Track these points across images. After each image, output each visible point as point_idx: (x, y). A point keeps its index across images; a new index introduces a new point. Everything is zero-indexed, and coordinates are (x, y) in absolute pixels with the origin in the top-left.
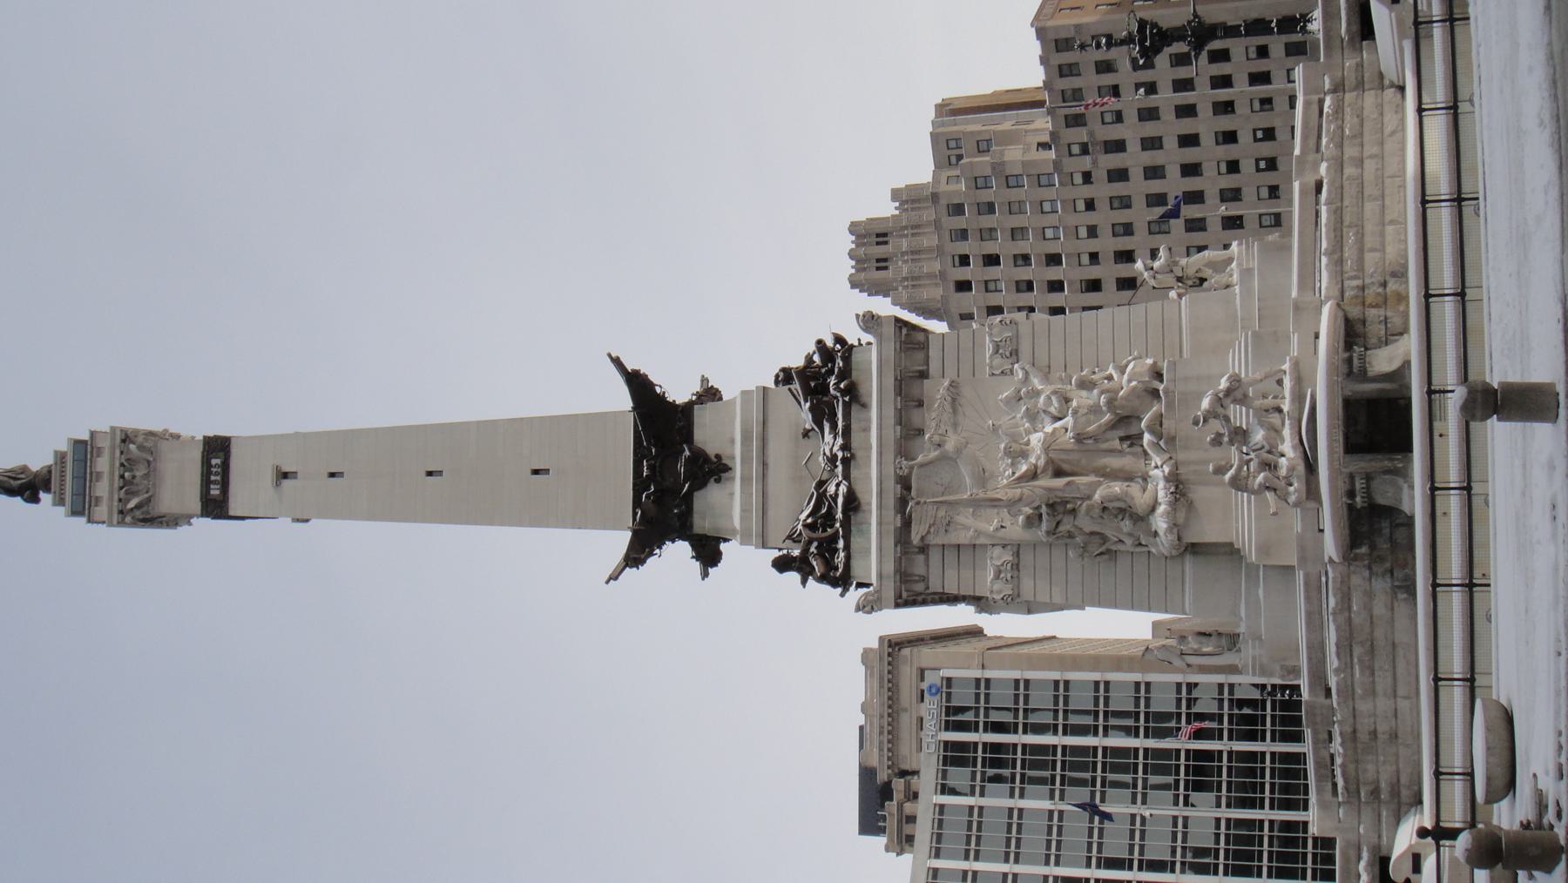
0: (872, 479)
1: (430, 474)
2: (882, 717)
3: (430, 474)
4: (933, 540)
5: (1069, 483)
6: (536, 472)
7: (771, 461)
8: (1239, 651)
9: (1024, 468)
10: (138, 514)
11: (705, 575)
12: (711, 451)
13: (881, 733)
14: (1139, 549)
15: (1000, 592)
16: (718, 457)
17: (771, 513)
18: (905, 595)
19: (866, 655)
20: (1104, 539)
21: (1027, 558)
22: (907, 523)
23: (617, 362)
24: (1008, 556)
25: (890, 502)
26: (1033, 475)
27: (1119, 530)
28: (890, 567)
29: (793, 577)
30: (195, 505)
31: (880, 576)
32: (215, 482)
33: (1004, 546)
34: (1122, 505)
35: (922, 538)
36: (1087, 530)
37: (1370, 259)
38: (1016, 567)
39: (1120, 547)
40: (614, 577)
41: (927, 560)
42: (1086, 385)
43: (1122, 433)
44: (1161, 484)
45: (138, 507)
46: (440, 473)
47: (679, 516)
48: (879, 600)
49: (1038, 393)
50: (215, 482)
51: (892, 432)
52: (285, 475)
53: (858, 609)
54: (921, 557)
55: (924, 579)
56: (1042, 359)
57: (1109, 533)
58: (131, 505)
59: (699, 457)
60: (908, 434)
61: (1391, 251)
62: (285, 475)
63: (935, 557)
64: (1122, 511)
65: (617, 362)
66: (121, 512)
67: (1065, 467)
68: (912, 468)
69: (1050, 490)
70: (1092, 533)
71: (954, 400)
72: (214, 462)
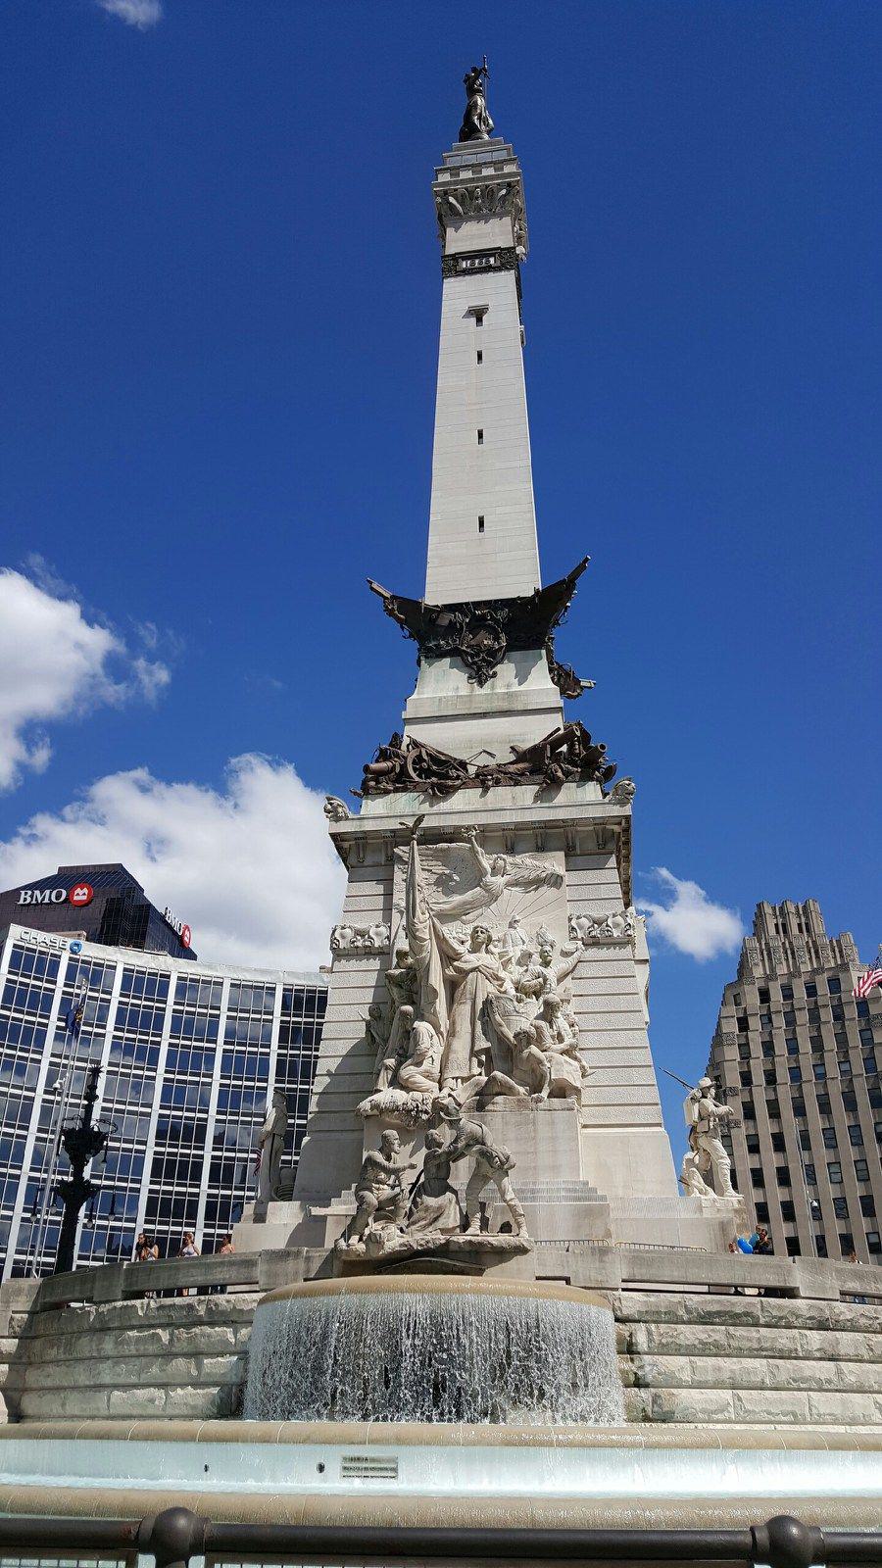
0: (463, 807)
1: (480, 435)
3: (480, 435)
18: (346, 845)
23: (581, 568)
26: (449, 957)
32: (473, 264)
33: (388, 938)
37: (677, 1363)
38: (369, 952)
41: (378, 865)
47: (438, 646)
50: (473, 264)
52: (479, 321)
56: (583, 970)
58: (451, 199)
60: (511, 839)
61: (688, 1398)
62: (479, 321)
65: (581, 568)
66: (446, 193)
68: (468, 841)
72: (492, 260)
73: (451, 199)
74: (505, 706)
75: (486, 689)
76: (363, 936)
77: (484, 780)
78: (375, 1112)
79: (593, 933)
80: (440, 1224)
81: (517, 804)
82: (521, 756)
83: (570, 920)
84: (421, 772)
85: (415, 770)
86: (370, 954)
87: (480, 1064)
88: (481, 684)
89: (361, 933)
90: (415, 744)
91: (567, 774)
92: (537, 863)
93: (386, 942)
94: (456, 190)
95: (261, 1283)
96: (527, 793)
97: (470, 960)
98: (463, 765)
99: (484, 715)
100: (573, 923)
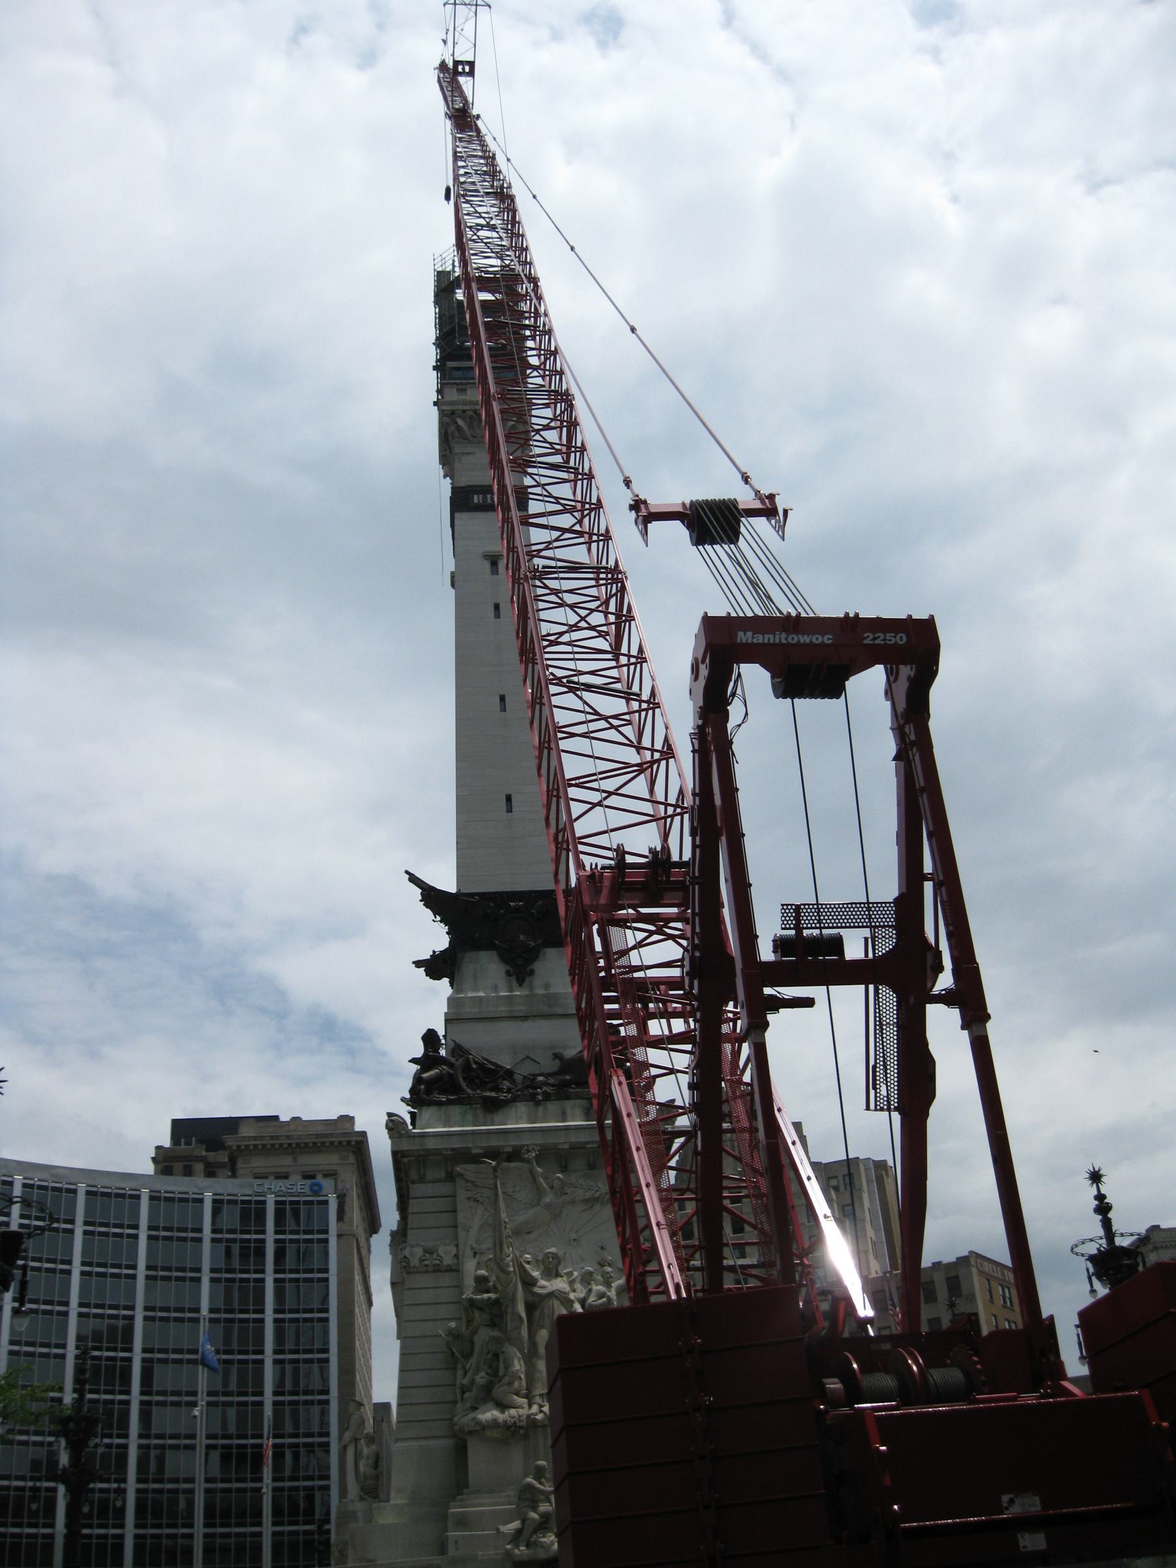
0: (517, 1121)
1: (502, 698)
2: (288, 1137)
3: (502, 698)
4: (460, 1183)
5: (520, 1318)
6: (509, 799)
7: (529, 1024)
8: (362, 1499)
9: (536, 1274)
10: (453, 428)
11: (418, 964)
12: (538, 966)
13: (272, 1138)
16: (532, 973)
17: (479, 1026)
18: (406, 1160)
19: (348, 1120)
20: (468, 1356)
21: (446, 1279)
22: (475, 1159)
24: (448, 1261)
25: (494, 1142)
27: (477, 1371)
28: (431, 1144)
29: (419, 1050)
30: (463, 481)
31: (423, 1136)
33: (456, 1256)
34: (501, 1373)
35: (461, 1175)
36: (476, 1338)
38: (437, 1269)
39: (460, 1373)
40: (413, 879)
41: (440, 1181)
44: (524, 1412)
45: (458, 427)
46: (503, 709)
48: (401, 1136)
49: (608, 1285)
51: (563, 1141)
53: (390, 1115)
54: (443, 1174)
55: (422, 1179)
57: (473, 1361)
58: (460, 422)
59: (532, 955)
63: (443, 1189)
64: (495, 1373)
66: (453, 413)
67: (537, 1314)
68: (528, 1161)
69: (513, 1300)
70: (472, 1343)
71: (597, 1199)
73: (460, 422)
76: (431, 1254)
77: (531, 1092)
78: (478, 1428)
84: (470, 1081)
85: (464, 1079)
86: (439, 1271)
94: (464, 411)
97: (546, 1285)
99: (525, 1018)
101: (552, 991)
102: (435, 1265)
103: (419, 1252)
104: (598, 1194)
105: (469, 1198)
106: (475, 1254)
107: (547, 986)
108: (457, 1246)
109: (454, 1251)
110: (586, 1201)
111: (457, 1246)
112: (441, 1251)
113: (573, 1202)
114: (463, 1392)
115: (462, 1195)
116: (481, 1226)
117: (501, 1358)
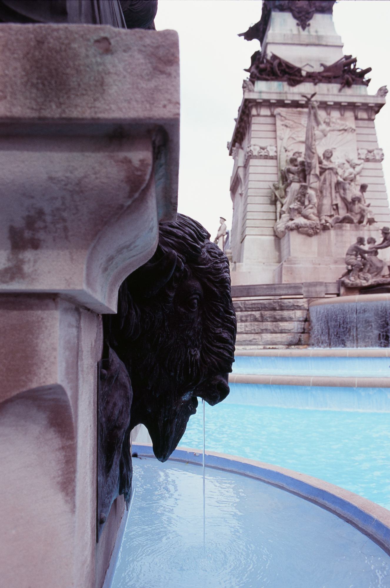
11: (240, 35)
12: (311, 22)
14: (278, 214)
15: (255, 150)
16: (309, 25)
21: (272, 162)
24: (272, 154)
33: (276, 152)
34: (307, 203)
38: (266, 157)
42: (363, 188)
43: (339, 205)
55: (258, 115)
63: (270, 120)
71: (345, 130)
74: (317, 42)
75: (305, 33)
79: (368, 157)
80: (382, 274)
81: (329, 92)
82: (327, 69)
83: (358, 150)
86: (267, 158)
87: (334, 209)
88: (304, 28)
89: (263, 148)
90: (274, 57)
91: (353, 80)
92: (343, 122)
93: (275, 154)
95: (305, 294)
96: (334, 87)
98: (299, 70)
99: (307, 45)
100: (360, 151)
101: (320, 34)
102: (265, 155)
103: (258, 149)
104: (346, 128)
105: (283, 125)
106: (286, 151)
107: (316, 32)
108: (276, 147)
109: (275, 149)
110: (340, 130)
111: (276, 147)
112: (268, 148)
113: (333, 130)
114: (281, 215)
115: (279, 123)
116: (289, 138)
117: (307, 196)
